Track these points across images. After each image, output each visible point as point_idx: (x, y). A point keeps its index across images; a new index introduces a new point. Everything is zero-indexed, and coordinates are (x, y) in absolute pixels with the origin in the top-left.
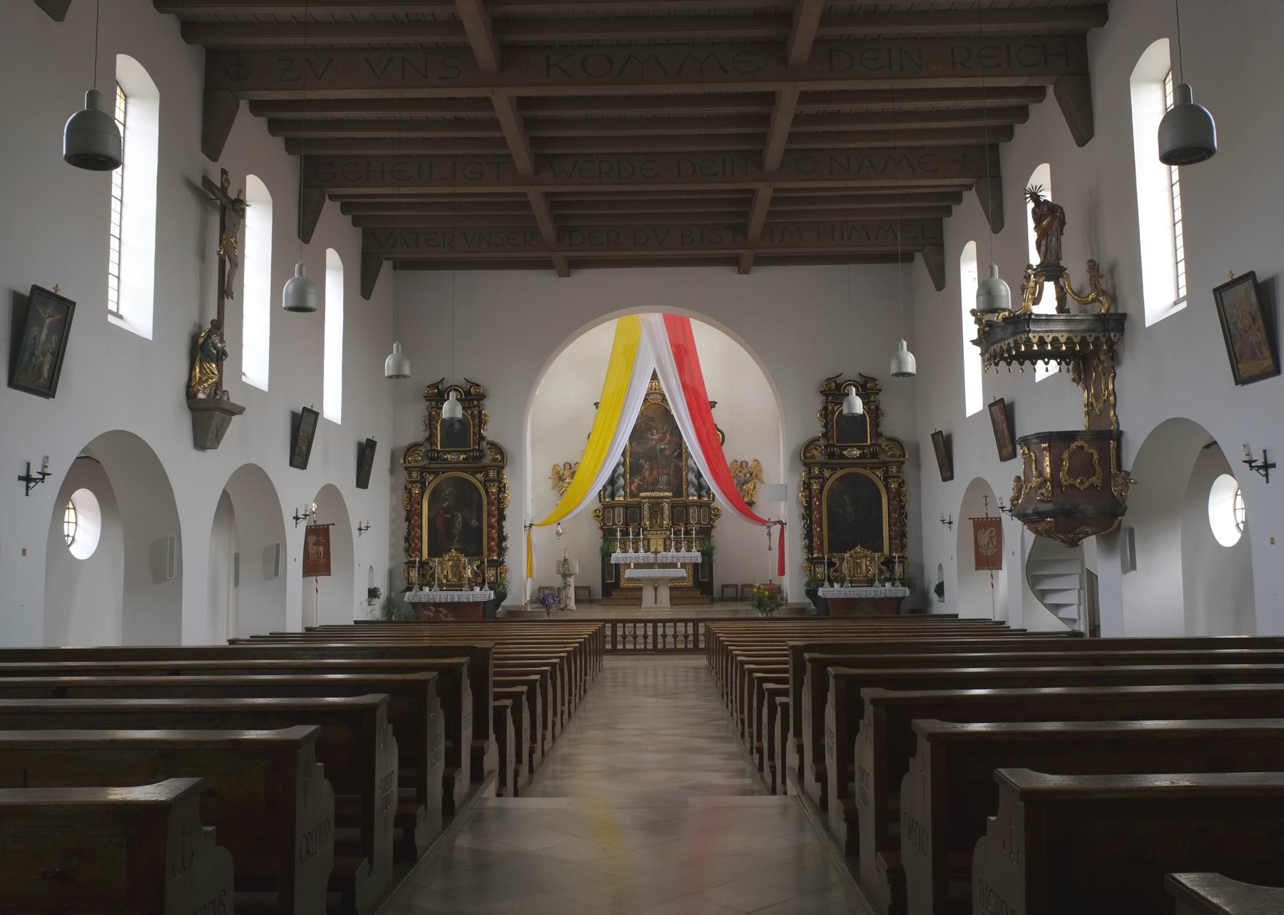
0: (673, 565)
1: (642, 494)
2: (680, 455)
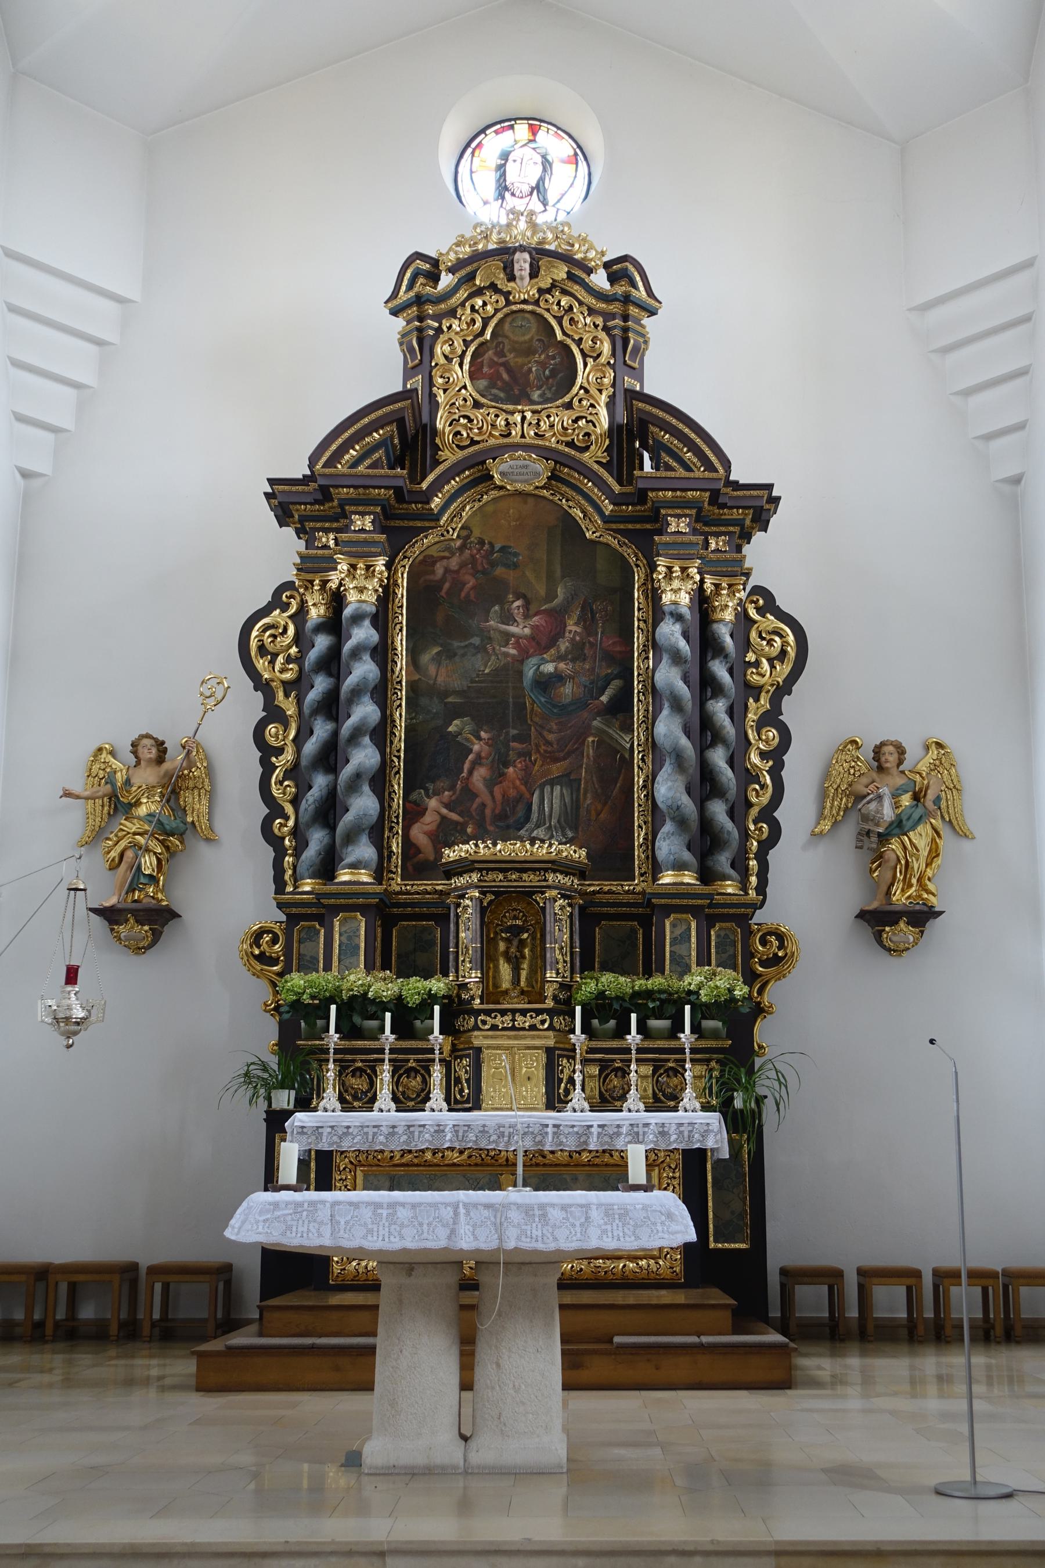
0: (603, 1171)
1: (451, 854)
2: (622, 706)
